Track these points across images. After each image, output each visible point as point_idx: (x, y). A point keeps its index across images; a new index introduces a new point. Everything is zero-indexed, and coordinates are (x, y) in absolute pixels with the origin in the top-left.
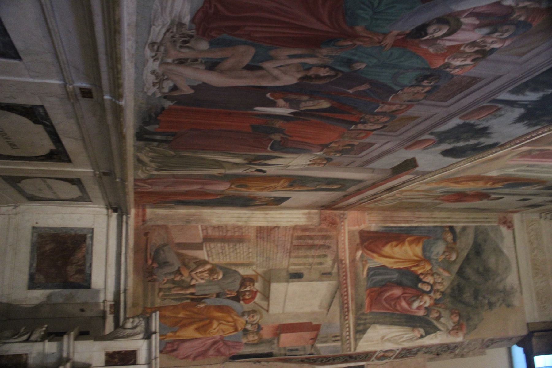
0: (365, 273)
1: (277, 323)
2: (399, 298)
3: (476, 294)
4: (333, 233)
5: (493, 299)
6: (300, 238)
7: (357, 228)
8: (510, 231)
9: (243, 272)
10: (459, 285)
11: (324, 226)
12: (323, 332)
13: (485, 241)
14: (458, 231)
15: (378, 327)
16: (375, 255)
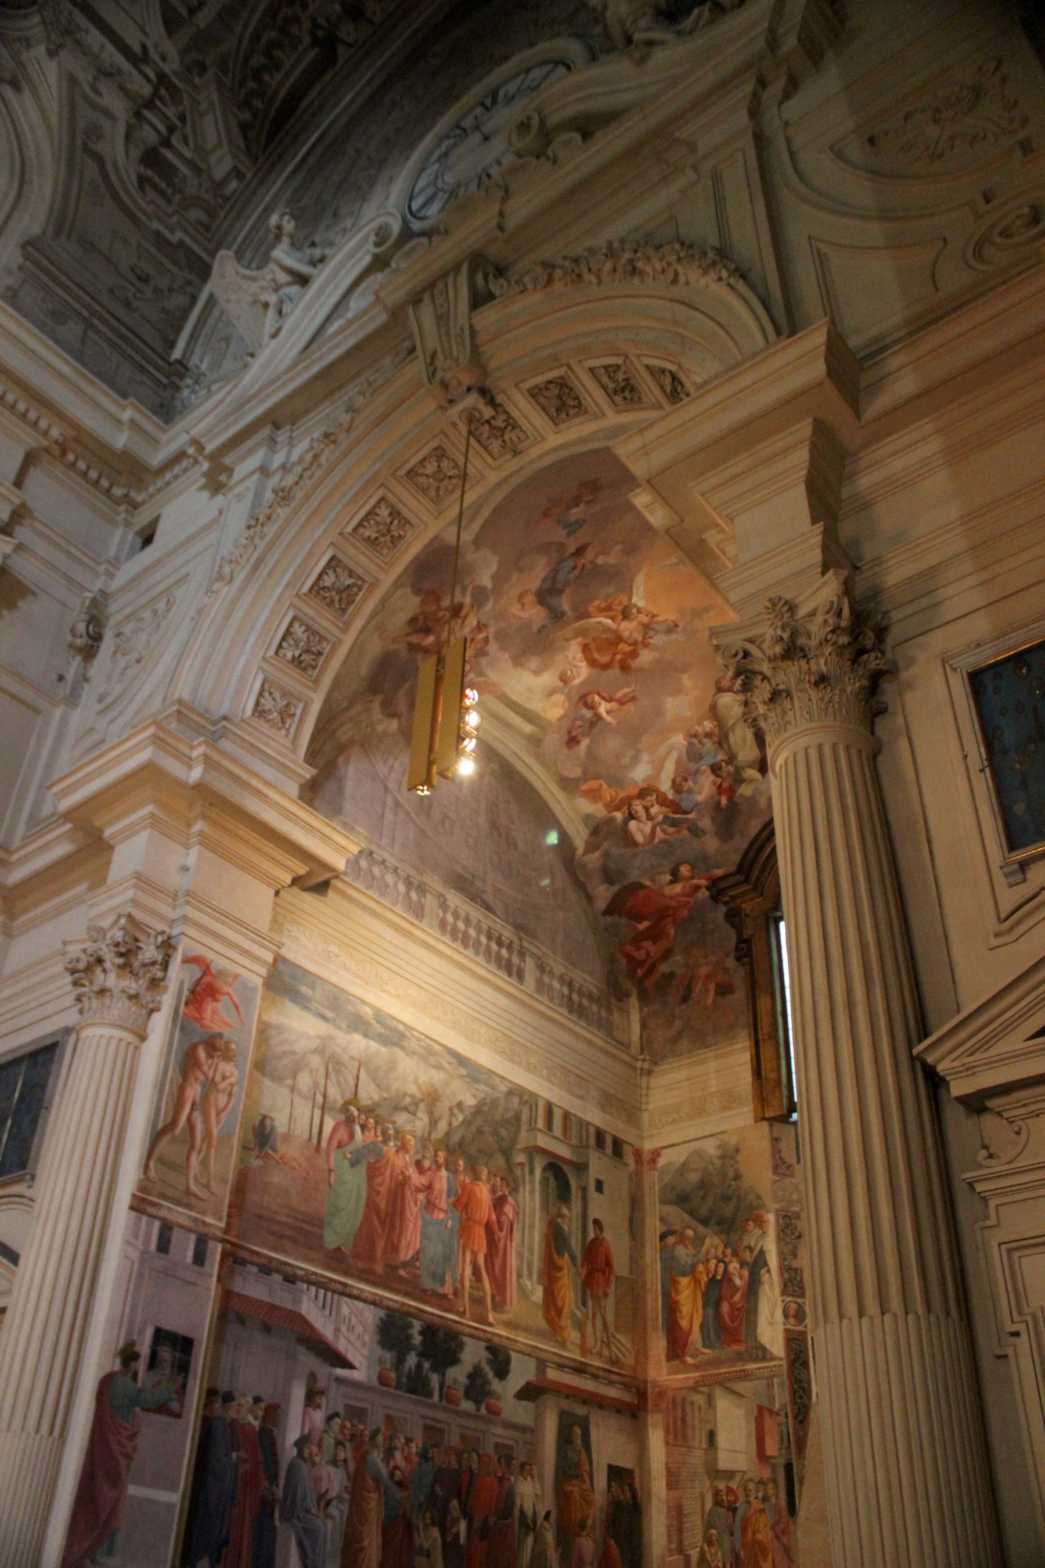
0: (708, 1351)
1: (756, 1460)
2: (730, 1304)
3: (727, 1198)
4: (670, 1394)
5: (731, 1174)
6: (676, 1436)
7: (664, 1363)
8: (664, 1152)
9: (709, 1504)
10: (718, 1224)
11: (663, 1406)
12: (765, 1402)
13: (673, 1189)
14: (664, 1228)
15: (759, 1330)
16: (690, 1339)
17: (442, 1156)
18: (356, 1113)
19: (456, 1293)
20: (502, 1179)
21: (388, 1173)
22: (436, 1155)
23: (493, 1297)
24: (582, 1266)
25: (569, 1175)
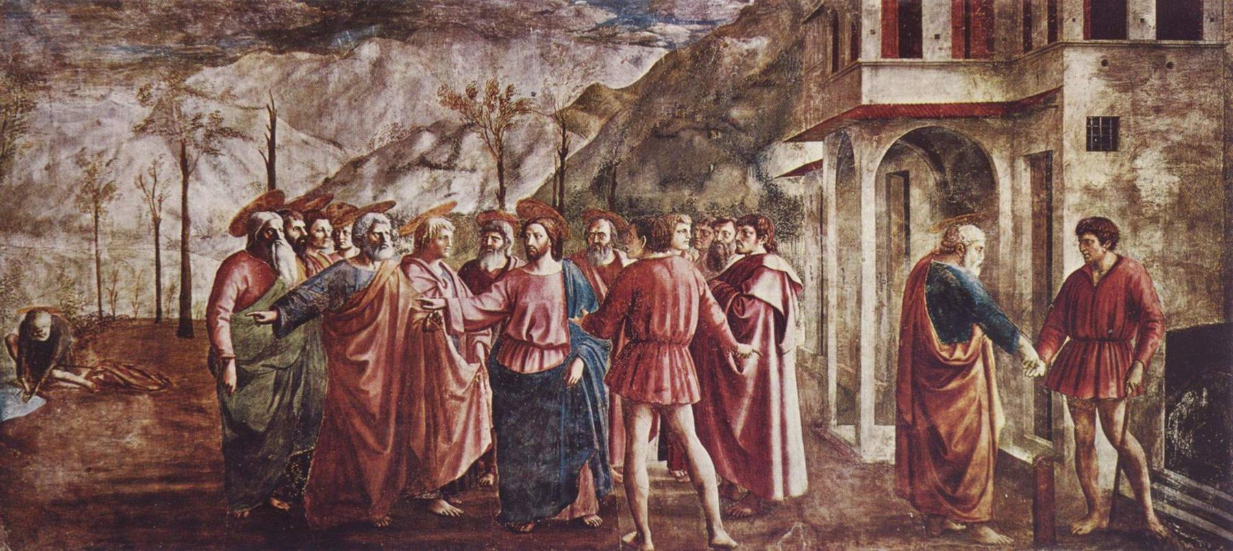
17: (539, 235)
18: (277, 222)
19: (609, 508)
20: (736, 225)
21: (384, 316)
22: (522, 235)
23: (726, 490)
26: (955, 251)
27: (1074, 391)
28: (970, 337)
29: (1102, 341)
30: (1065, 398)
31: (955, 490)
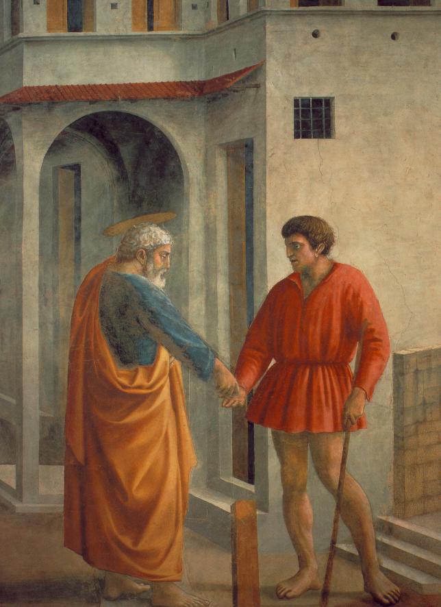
24: (238, 371)
25: (172, 131)
26: (135, 257)
27: (284, 425)
28: (154, 359)
29: (312, 364)
30: (269, 431)
31: (136, 543)
